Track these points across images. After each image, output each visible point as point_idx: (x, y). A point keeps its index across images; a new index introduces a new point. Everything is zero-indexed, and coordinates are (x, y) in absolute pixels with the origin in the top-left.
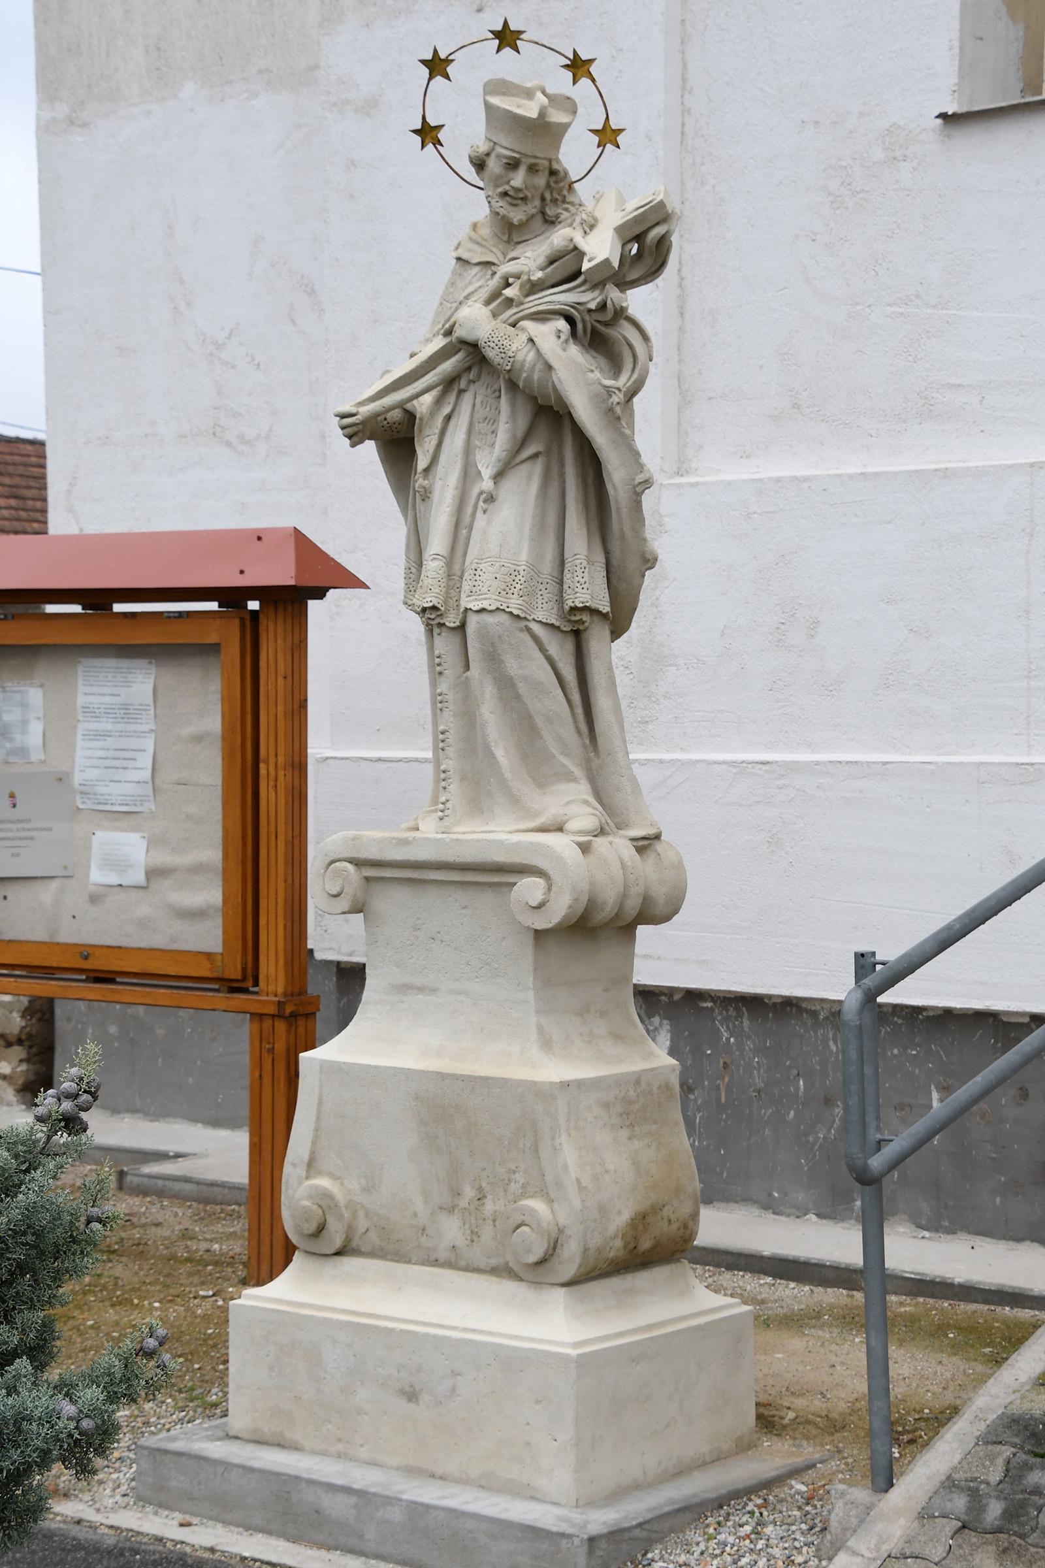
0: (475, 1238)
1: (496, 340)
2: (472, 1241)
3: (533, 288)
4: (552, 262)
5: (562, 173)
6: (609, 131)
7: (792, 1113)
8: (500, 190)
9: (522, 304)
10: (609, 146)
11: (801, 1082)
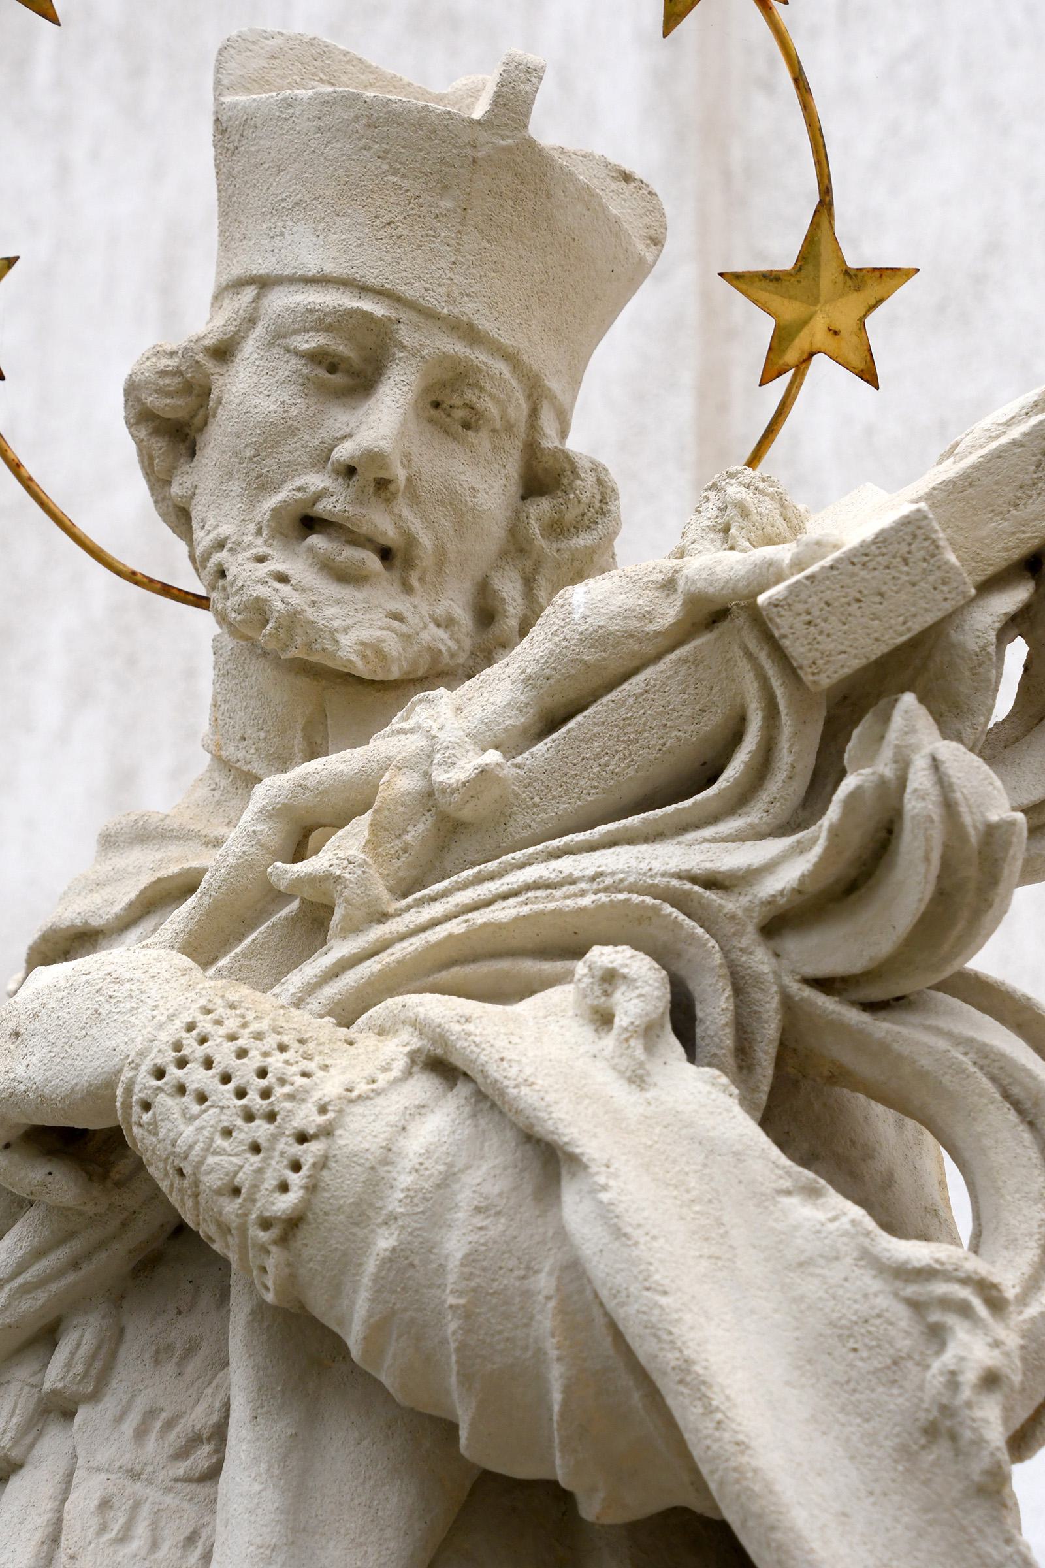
1: (224, 1055)
3: (453, 833)
4: (551, 722)
5: (586, 487)
6: (828, 276)
9: (383, 917)
10: (825, 373)
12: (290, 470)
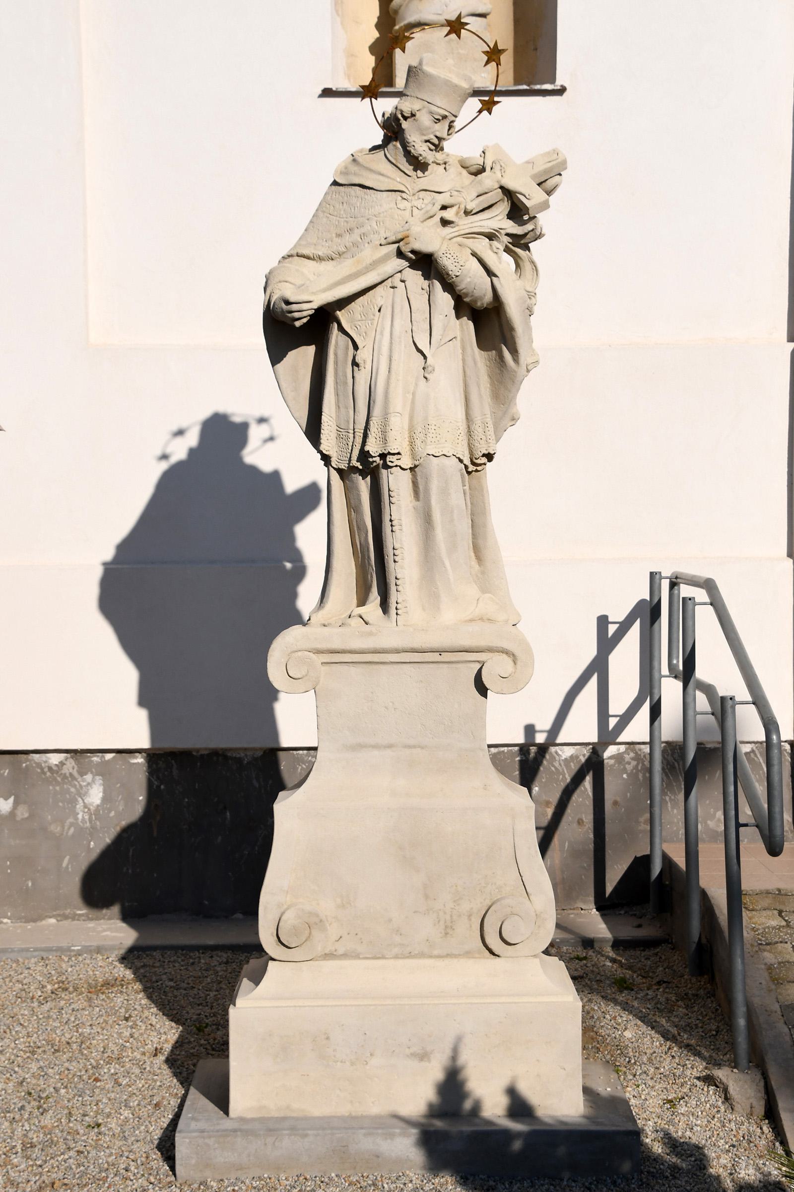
0: (449, 931)
2: (446, 934)
7: (220, 838)
8: (426, 138)
11: (228, 814)
12: (429, 134)
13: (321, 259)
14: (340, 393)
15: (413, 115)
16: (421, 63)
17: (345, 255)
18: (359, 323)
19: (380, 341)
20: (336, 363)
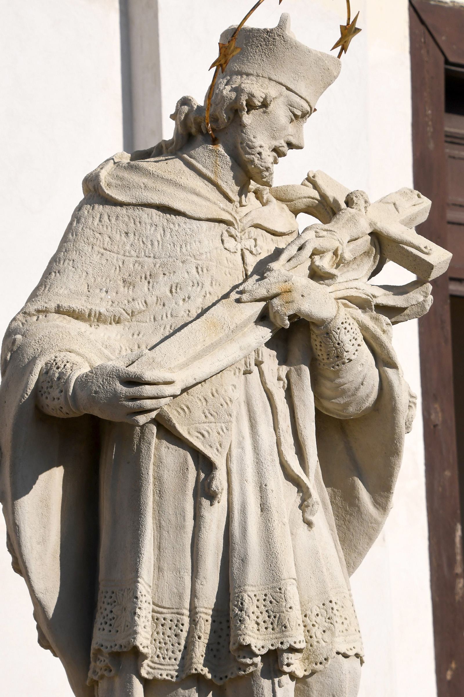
13: (100, 319)
14: (165, 544)
15: (265, 105)
16: (283, 23)
17: (139, 317)
18: (206, 426)
19: (241, 460)
20: (160, 493)
